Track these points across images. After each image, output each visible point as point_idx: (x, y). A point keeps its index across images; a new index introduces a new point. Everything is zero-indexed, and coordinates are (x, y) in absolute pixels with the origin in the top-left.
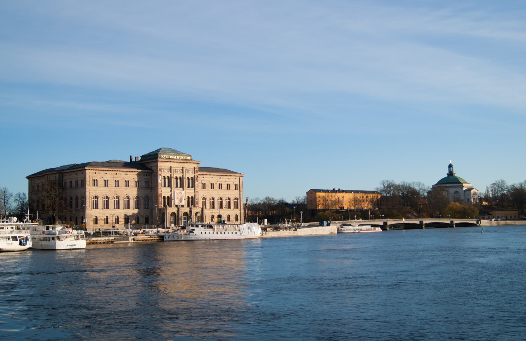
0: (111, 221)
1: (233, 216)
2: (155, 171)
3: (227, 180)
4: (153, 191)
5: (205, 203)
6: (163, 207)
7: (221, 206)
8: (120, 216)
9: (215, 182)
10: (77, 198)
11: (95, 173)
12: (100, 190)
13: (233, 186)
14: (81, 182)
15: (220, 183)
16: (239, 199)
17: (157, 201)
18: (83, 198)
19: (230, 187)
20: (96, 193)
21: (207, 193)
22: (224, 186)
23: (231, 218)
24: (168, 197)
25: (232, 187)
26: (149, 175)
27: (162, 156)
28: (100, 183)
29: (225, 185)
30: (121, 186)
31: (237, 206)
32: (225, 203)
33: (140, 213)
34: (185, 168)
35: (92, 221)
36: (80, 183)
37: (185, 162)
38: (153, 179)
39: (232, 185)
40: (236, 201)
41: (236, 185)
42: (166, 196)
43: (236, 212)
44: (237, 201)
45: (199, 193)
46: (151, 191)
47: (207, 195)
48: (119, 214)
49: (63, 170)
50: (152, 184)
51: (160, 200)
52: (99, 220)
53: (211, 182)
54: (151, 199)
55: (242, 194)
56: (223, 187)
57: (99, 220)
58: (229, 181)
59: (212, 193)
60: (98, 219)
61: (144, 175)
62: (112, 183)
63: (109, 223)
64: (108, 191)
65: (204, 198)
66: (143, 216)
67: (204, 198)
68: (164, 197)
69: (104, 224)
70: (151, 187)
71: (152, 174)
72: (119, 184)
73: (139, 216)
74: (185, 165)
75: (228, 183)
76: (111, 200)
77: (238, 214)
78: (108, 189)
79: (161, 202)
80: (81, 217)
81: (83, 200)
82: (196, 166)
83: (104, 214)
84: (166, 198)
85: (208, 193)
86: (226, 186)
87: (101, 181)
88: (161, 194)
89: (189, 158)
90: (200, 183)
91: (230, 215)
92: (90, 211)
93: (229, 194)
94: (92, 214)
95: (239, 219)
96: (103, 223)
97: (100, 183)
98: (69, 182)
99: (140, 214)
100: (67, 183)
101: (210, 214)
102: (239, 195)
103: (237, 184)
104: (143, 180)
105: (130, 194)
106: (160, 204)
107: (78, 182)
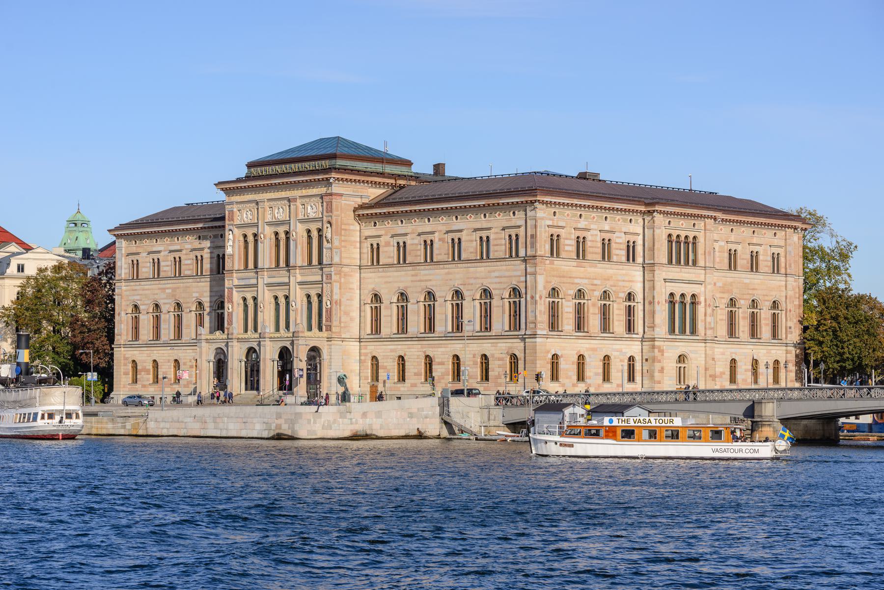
9: (436, 234)
12: (143, 290)
13: (503, 242)
19: (492, 248)
21: (410, 278)
25: (499, 248)
32: (472, 310)
39: (499, 242)
41: (514, 242)
48: (180, 355)
60: (138, 368)
64: (159, 289)
75: (484, 234)
85: (414, 278)
90: (387, 244)
94: (127, 356)
97: (144, 270)
101: (420, 353)
102: (523, 279)
106: (228, 324)
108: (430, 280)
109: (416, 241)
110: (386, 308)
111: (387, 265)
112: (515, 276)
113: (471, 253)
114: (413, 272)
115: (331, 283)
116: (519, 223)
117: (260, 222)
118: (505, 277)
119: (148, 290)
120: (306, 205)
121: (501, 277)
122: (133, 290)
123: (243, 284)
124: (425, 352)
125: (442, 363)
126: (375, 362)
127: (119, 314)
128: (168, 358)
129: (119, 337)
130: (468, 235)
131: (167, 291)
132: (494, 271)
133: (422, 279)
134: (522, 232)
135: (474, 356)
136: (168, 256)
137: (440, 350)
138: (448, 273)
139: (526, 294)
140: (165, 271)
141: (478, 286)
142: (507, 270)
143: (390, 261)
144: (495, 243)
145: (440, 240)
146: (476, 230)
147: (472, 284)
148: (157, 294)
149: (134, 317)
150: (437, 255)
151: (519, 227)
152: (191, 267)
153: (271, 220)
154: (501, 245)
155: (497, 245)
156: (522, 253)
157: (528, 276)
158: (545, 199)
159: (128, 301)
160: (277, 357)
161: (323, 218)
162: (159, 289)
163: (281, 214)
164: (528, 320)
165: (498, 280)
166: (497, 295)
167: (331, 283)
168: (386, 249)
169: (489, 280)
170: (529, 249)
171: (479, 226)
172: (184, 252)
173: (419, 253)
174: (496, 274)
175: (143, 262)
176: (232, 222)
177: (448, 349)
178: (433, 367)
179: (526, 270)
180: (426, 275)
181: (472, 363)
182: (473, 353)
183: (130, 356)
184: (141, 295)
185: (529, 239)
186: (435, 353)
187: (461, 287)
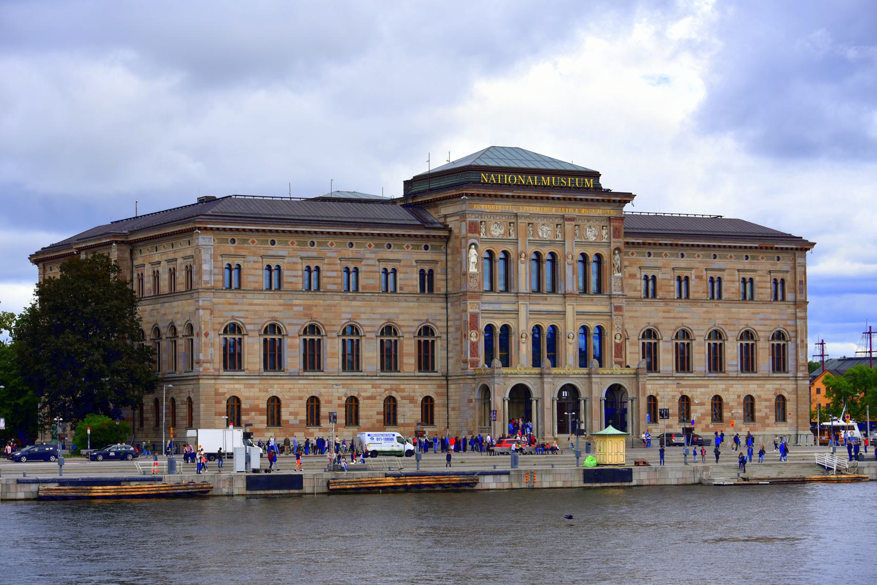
0: (291, 414)
1: (766, 400)
2: (456, 231)
3: (746, 264)
4: (449, 305)
5: (650, 353)
6: (483, 366)
7: (716, 362)
8: (326, 398)
9: (693, 271)
10: (173, 328)
11: (233, 241)
13: (769, 285)
14: (184, 273)
15: (716, 275)
16: (792, 334)
17: (461, 342)
18: (192, 334)
19: (756, 290)
20: (236, 314)
21: (661, 314)
22: (732, 287)
23: (757, 407)
24: (506, 329)
25: (764, 290)
26: (434, 248)
27: (482, 174)
28: (251, 278)
29: (733, 281)
30: (329, 287)
31: (779, 364)
32: (732, 353)
33: (402, 387)
34: (571, 219)
35: (221, 414)
36: (181, 276)
37: (570, 199)
38: (449, 264)
39: (763, 285)
40: (779, 345)
41: (779, 285)
42: (498, 324)
43: (778, 386)
44: (782, 343)
45: (627, 314)
46: (444, 305)
47: (661, 320)
48: (323, 390)
49: (132, 232)
50: (447, 280)
51: (474, 340)
52: (246, 410)
53: (678, 273)
54: (444, 336)
55: (801, 318)
56: (726, 290)
57: (248, 412)
58: (753, 267)
59: (685, 315)
60: (243, 406)
61: (417, 247)
62: (294, 276)
63: (282, 424)
64: (280, 305)
65: (650, 333)
66: (412, 400)
67: (649, 331)
68: (490, 328)
69: (266, 425)
70: (443, 290)
71: (447, 243)
72: (323, 281)
73: (398, 399)
74: (571, 211)
75: (748, 276)
76: (294, 337)
77: (785, 395)
78: (282, 301)
79: (474, 346)
80: (185, 400)
81: (192, 340)
82: (612, 212)
83: (267, 391)
84: (498, 331)
85: (667, 315)
86: (738, 285)
87: (253, 272)
88: (474, 317)
89: (589, 183)
90: (632, 276)
91: (754, 395)
92: (216, 377)
93: (750, 320)
94: (221, 390)
95: (793, 413)
96: (262, 422)
97: (251, 278)
98: (151, 273)
99: (403, 391)
100: (145, 279)
101: (676, 393)
103: (783, 281)
104: (414, 264)
105: (363, 316)
106: (472, 355)
107: (177, 274)
108: (686, 318)
109: (668, 276)
110: (632, 344)
111: (634, 298)
112: (783, 320)
113: (733, 293)
114: (666, 308)
115: (622, 316)
116: (785, 268)
117: (520, 239)
118: (771, 320)
119: (260, 305)
120: (582, 226)
121: (766, 319)
122: (230, 304)
123: (491, 308)
124: (681, 392)
125: (702, 404)
126: (652, 402)
127: (207, 335)
128: (299, 394)
129: (208, 365)
130: (729, 275)
131: (295, 308)
132: (758, 313)
133: (676, 316)
134: (788, 278)
135: (739, 397)
136: (297, 263)
137: (699, 390)
138: (707, 312)
139: (796, 337)
140: (291, 283)
141: (741, 327)
142: (772, 313)
143: (637, 294)
144: (760, 285)
145: (697, 277)
146: (738, 270)
147: (734, 325)
148: (277, 311)
149: (712, 346)
150: (693, 292)
151: (787, 272)
152: (339, 281)
153: (532, 238)
154: (766, 288)
155: (761, 288)
156: (789, 296)
157: (798, 320)
158: (680, 243)
159: (220, 317)
160: (604, 395)
161: (610, 243)
162: (280, 305)
163: (545, 232)
164: (799, 364)
165: (762, 322)
166: (762, 337)
167: (622, 316)
168: (631, 281)
169: (753, 322)
170: (798, 295)
171: (740, 267)
172: (326, 261)
173: (672, 289)
174: (761, 316)
175: (249, 268)
176: (477, 235)
177: (707, 390)
178: (692, 408)
179: (795, 314)
180: (680, 312)
181: (735, 404)
182: (737, 393)
183: (225, 390)
184: (247, 311)
185: (798, 285)
186: (694, 393)
187: (723, 327)
